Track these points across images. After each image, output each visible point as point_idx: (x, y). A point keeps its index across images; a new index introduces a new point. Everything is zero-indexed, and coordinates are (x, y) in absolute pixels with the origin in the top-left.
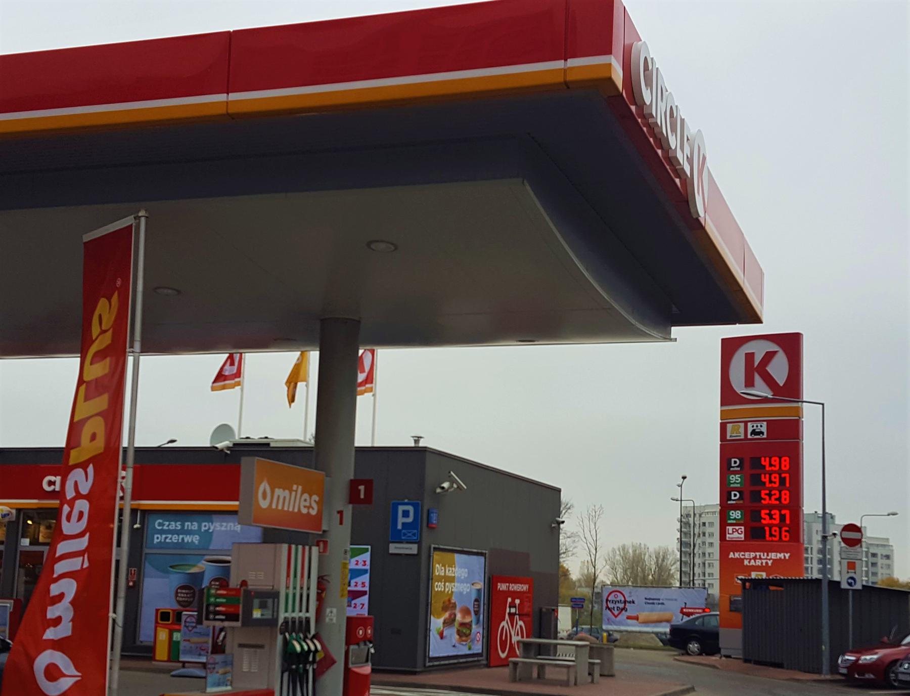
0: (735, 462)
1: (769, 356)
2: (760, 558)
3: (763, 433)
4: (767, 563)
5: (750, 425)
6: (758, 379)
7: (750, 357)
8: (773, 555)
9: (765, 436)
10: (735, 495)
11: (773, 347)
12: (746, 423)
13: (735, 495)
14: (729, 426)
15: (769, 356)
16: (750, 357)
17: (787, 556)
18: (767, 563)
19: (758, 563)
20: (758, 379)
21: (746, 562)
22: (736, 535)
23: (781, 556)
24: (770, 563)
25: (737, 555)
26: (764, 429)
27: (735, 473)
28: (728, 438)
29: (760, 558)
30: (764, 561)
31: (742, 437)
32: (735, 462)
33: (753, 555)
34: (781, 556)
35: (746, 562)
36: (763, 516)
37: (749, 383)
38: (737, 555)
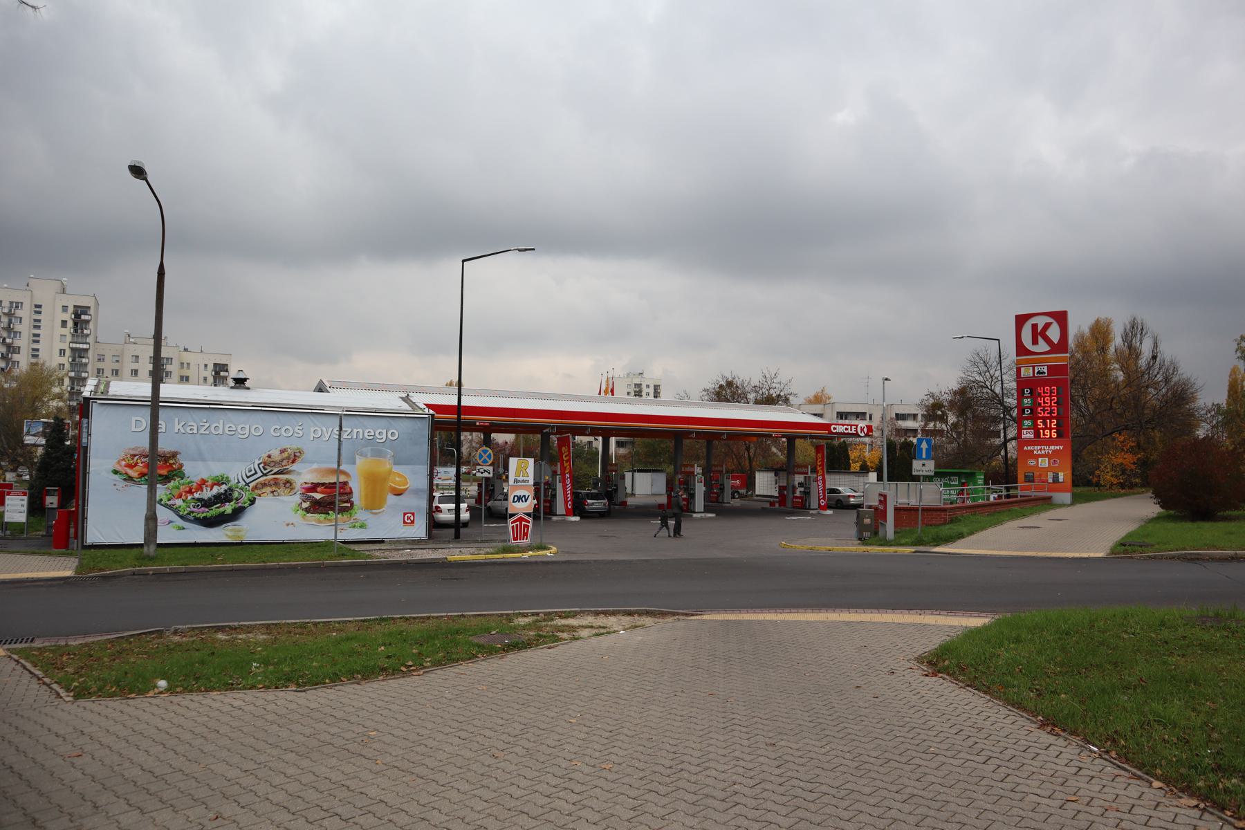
0: (1027, 391)
1: (1047, 326)
2: (1044, 449)
3: (1045, 373)
4: (1048, 452)
5: (1036, 368)
6: (1040, 339)
7: (1035, 326)
8: (1052, 448)
9: (1046, 374)
10: (1027, 411)
11: (1049, 320)
12: (1034, 367)
13: (1027, 411)
14: (1023, 369)
15: (1047, 326)
16: (1035, 326)
17: (1061, 447)
18: (1048, 452)
19: (1043, 452)
20: (1040, 339)
21: (1035, 452)
22: (1028, 435)
23: (1058, 448)
24: (1050, 452)
25: (1029, 448)
26: (1045, 370)
27: (1027, 398)
28: (1022, 376)
29: (1044, 449)
30: (1047, 451)
31: (1032, 375)
32: (1027, 391)
33: (1039, 447)
34: (1058, 448)
35: (1035, 452)
36: (1041, 424)
37: (1035, 342)
38: (1029, 448)
